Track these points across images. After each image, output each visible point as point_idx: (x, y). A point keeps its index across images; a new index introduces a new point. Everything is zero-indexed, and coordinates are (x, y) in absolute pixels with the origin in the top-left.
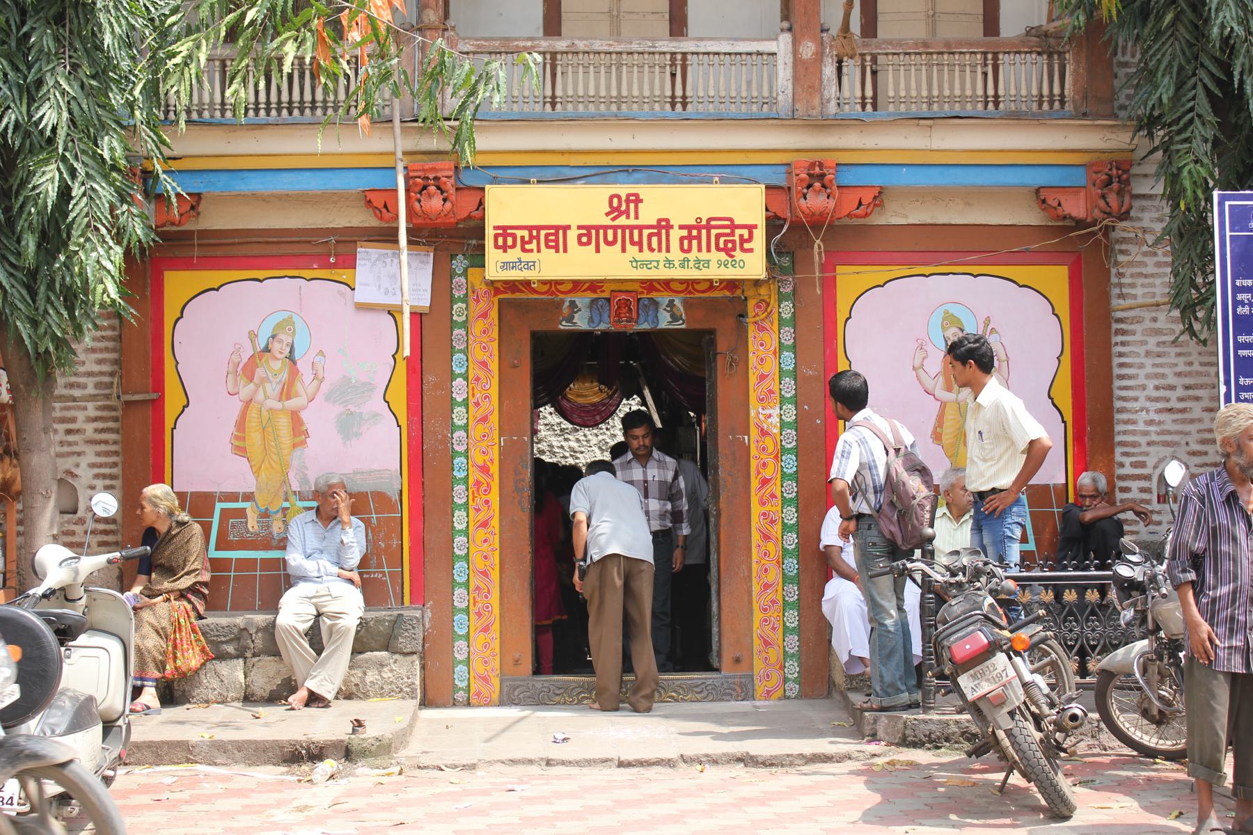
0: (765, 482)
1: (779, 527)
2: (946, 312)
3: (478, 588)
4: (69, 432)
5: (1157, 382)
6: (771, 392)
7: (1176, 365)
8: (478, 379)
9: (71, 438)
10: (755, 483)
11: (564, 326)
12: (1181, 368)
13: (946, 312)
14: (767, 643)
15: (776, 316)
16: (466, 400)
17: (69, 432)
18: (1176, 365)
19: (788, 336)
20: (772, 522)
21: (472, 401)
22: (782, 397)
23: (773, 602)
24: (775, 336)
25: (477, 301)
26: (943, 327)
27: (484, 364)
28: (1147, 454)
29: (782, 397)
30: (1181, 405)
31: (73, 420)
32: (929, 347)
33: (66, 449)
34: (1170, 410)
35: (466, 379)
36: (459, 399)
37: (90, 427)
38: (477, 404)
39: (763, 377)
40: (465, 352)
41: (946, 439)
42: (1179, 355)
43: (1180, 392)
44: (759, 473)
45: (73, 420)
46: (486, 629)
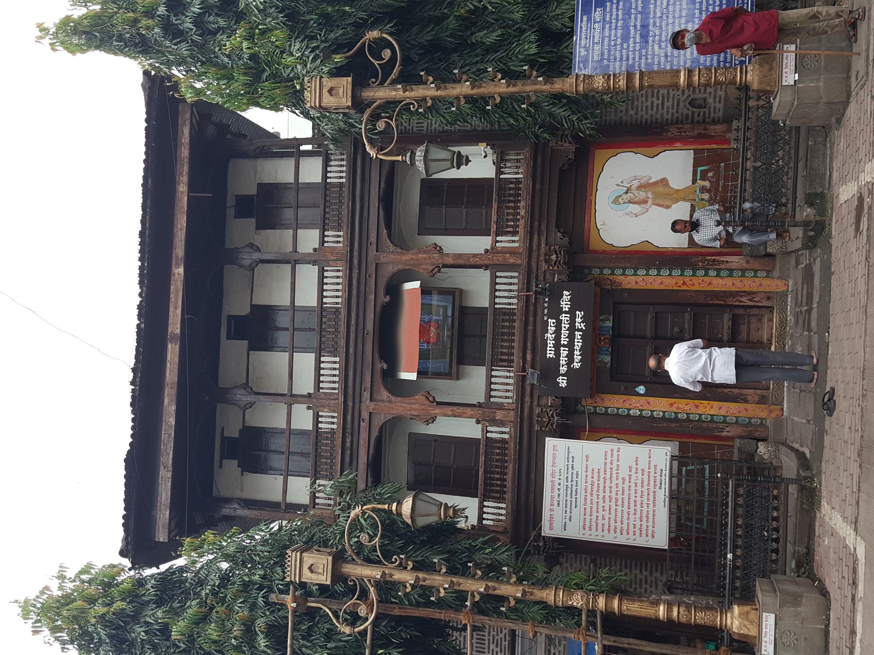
0: (684, 283)
1: (706, 279)
2: (612, 203)
3: (727, 412)
4: (646, 582)
5: (650, 110)
6: (643, 279)
7: (642, 101)
8: (631, 405)
9: (649, 581)
10: (684, 288)
11: (609, 365)
12: (644, 99)
13: (612, 203)
14: (761, 285)
15: (609, 277)
16: (640, 410)
17: (646, 582)
18: (642, 101)
19: (619, 272)
20: (703, 281)
21: (640, 408)
22: (645, 275)
23: (741, 281)
24: (619, 277)
25: (596, 402)
26: (620, 204)
27: (624, 401)
28: (682, 113)
29: (645, 275)
30: (661, 98)
31: (641, 580)
32: (627, 211)
33: (654, 585)
34: (663, 104)
35: (630, 409)
36: (639, 413)
37: (644, 573)
38: (642, 406)
39: (636, 283)
40: (618, 409)
41: (668, 203)
42: (638, 101)
43: (655, 99)
44: (680, 286)
45: (641, 580)
46: (746, 410)
